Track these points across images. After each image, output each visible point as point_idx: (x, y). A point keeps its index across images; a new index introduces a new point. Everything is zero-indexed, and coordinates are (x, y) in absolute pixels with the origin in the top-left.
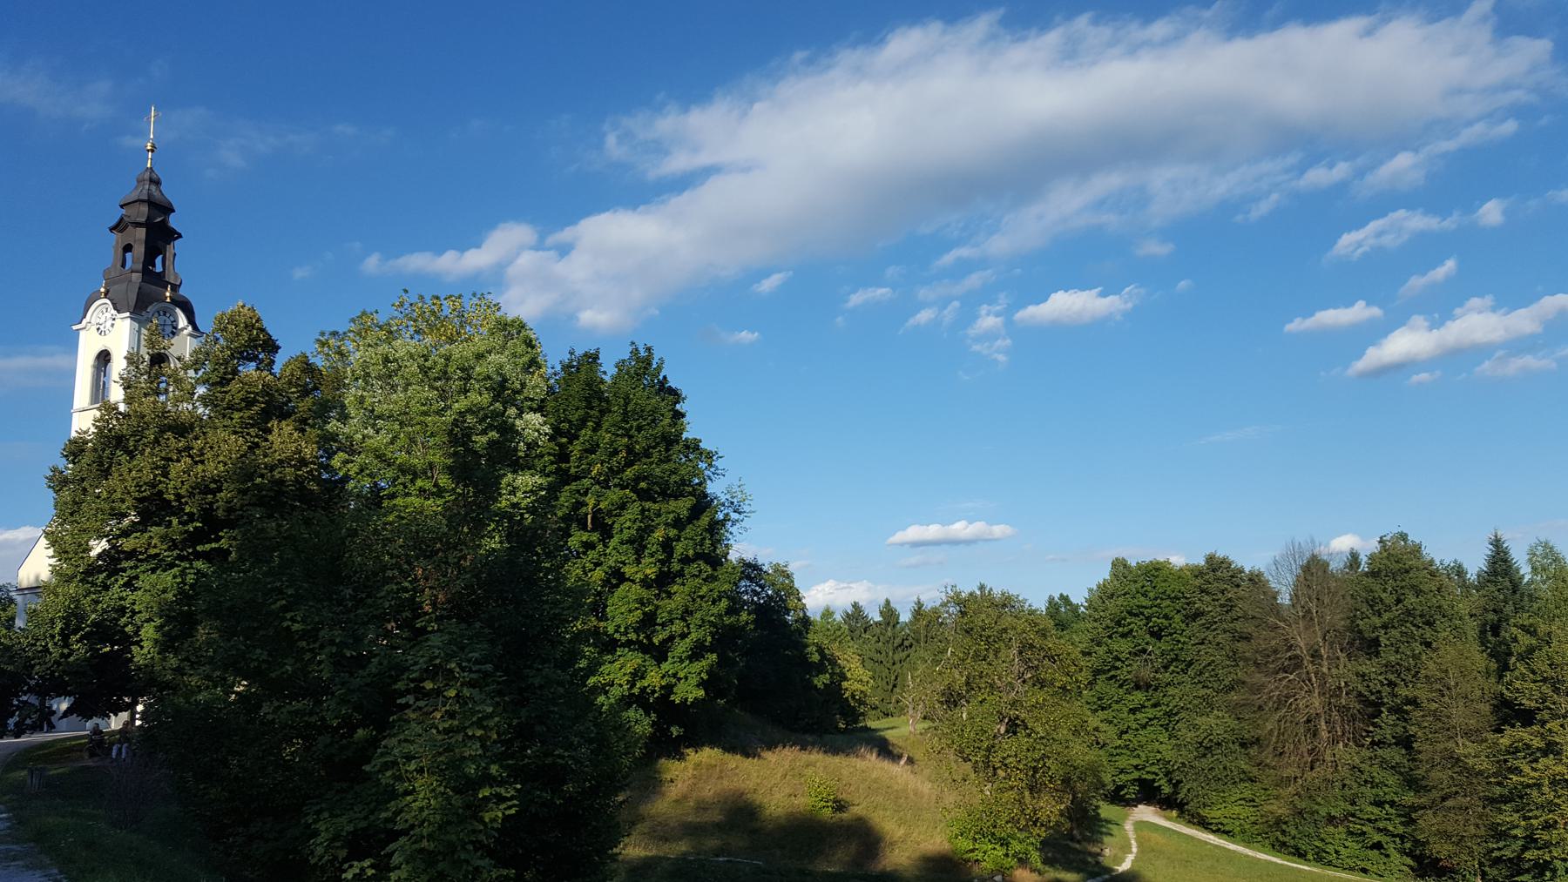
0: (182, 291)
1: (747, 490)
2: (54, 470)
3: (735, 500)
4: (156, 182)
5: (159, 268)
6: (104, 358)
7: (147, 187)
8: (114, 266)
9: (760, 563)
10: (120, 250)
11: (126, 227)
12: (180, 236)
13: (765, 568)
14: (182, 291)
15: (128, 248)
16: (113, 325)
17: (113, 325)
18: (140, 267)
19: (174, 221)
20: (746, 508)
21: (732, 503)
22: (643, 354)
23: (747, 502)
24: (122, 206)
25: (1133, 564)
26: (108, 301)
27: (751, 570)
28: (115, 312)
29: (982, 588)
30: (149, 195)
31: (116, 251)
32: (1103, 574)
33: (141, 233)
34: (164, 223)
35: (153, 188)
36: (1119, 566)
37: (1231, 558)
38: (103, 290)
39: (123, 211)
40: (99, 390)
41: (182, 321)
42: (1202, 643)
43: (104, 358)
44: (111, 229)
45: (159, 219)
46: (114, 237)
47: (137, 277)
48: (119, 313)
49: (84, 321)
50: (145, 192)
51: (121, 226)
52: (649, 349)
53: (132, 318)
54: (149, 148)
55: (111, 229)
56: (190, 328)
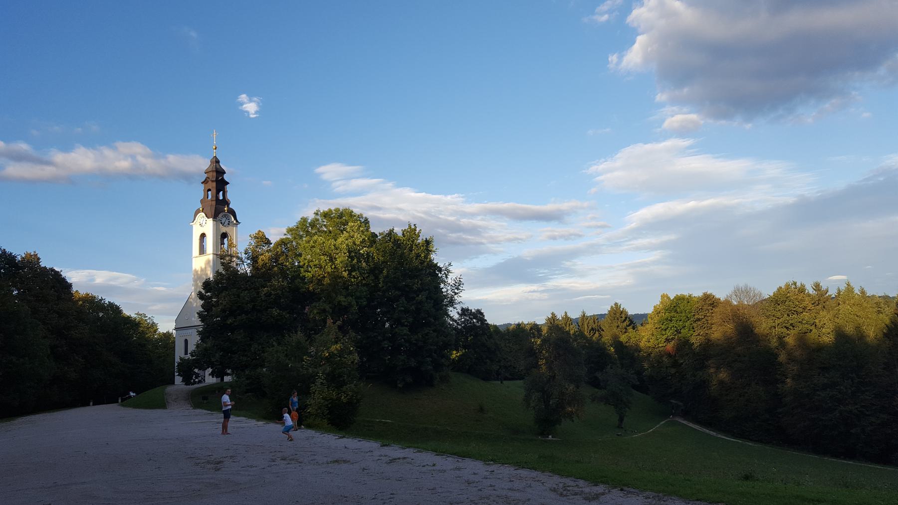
0: (231, 206)
1: (461, 279)
2: (200, 292)
3: (457, 284)
4: (218, 162)
5: (221, 198)
6: (203, 236)
7: (215, 165)
8: (204, 198)
9: (469, 308)
10: (206, 191)
11: (208, 181)
12: (228, 183)
13: (473, 311)
14: (231, 206)
15: (209, 190)
16: (206, 223)
17: (206, 223)
18: (214, 199)
19: (226, 177)
20: (461, 288)
21: (456, 285)
22: (413, 227)
23: (461, 286)
24: (205, 173)
25: (672, 299)
26: (203, 214)
27: (465, 312)
28: (205, 217)
29: (616, 304)
30: (216, 168)
31: (204, 190)
32: (657, 301)
33: (214, 184)
34: (223, 179)
35: (217, 164)
36: (663, 296)
37: (714, 294)
38: (201, 209)
39: (206, 175)
40: (202, 251)
41: (233, 219)
42: (699, 335)
43: (203, 236)
44: (202, 183)
45: (220, 178)
46: (203, 185)
47: (214, 203)
48: (208, 218)
49: (195, 221)
50: (214, 167)
51: (206, 182)
52: (415, 225)
53: (213, 221)
54: (214, 148)
55: (202, 183)
56: (235, 222)
